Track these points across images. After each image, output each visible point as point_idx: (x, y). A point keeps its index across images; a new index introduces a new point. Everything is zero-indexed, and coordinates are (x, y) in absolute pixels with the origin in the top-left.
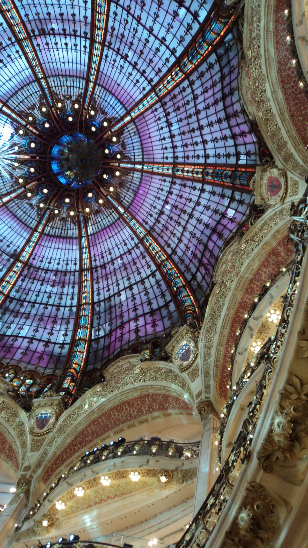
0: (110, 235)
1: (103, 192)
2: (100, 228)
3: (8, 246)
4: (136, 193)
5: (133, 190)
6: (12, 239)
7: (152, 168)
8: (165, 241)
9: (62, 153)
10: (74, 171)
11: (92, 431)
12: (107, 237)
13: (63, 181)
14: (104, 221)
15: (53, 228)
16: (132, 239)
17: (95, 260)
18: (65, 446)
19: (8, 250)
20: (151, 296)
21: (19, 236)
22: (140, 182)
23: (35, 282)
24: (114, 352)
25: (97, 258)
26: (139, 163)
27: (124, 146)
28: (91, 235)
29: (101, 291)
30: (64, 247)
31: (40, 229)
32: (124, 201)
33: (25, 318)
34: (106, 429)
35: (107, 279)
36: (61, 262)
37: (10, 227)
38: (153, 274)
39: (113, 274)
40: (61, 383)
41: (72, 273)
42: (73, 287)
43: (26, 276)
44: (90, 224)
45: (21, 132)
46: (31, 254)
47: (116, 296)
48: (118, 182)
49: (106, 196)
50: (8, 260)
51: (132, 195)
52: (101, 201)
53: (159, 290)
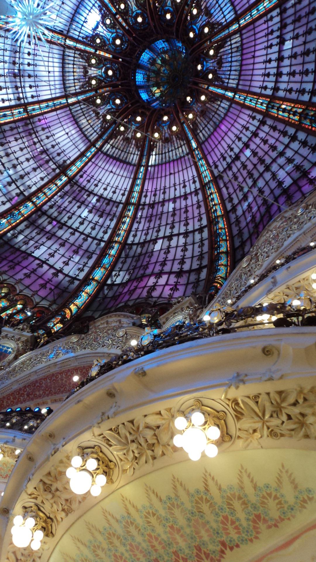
0: (172, 171)
1: (181, 117)
2: (164, 160)
3: (59, 154)
4: (217, 127)
5: (215, 123)
6: (65, 148)
7: (245, 99)
8: (229, 194)
9: (153, 62)
10: (161, 89)
11: (47, 387)
12: (168, 173)
13: (144, 96)
14: (171, 153)
15: (113, 147)
16: (194, 182)
17: (146, 196)
18: (8, 392)
19: (58, 158)
20: (189, 254)
21: (74, 147)
22: (226, 115)
23: (83, 207)
24: (118, 305)
25: (149, 194)
26: (232, 90)
27: (220, 63)
28: (151, 166)
29: (139, 233)
30: (117, 172)
31: (98, 145)
32: (201, 134)
33: (47, 238)
34: (62, 389)
35: (150, 221)
36: (109, 188)
37: (67, 134)
38: (201, 230)
39: (158, 217)
40: (49, 320)
41: (116, 204)
42: (111, 220)
43: (66, 193)
44: (154, 153)
45: (108, 22)
46: (80, 170)
47: (151, 243)
48: (200, 109)
49: (182, 124)
50: (54, 170)
51: (212, 129)
52: (174, 128)
53: (200, 250)
